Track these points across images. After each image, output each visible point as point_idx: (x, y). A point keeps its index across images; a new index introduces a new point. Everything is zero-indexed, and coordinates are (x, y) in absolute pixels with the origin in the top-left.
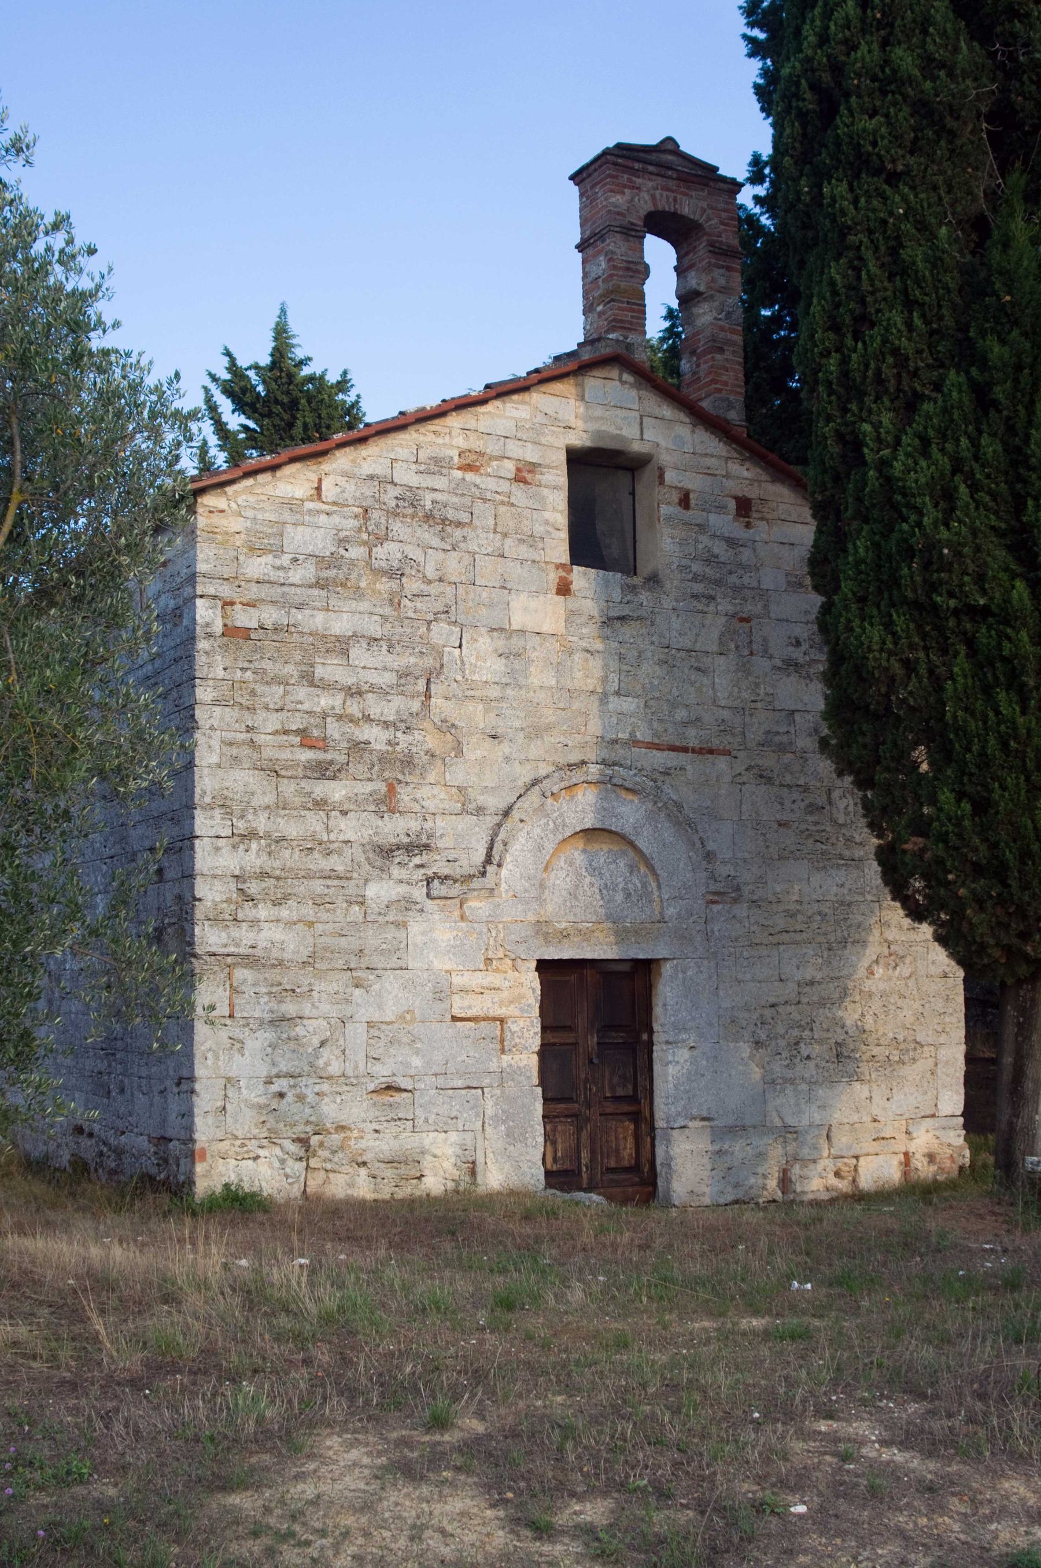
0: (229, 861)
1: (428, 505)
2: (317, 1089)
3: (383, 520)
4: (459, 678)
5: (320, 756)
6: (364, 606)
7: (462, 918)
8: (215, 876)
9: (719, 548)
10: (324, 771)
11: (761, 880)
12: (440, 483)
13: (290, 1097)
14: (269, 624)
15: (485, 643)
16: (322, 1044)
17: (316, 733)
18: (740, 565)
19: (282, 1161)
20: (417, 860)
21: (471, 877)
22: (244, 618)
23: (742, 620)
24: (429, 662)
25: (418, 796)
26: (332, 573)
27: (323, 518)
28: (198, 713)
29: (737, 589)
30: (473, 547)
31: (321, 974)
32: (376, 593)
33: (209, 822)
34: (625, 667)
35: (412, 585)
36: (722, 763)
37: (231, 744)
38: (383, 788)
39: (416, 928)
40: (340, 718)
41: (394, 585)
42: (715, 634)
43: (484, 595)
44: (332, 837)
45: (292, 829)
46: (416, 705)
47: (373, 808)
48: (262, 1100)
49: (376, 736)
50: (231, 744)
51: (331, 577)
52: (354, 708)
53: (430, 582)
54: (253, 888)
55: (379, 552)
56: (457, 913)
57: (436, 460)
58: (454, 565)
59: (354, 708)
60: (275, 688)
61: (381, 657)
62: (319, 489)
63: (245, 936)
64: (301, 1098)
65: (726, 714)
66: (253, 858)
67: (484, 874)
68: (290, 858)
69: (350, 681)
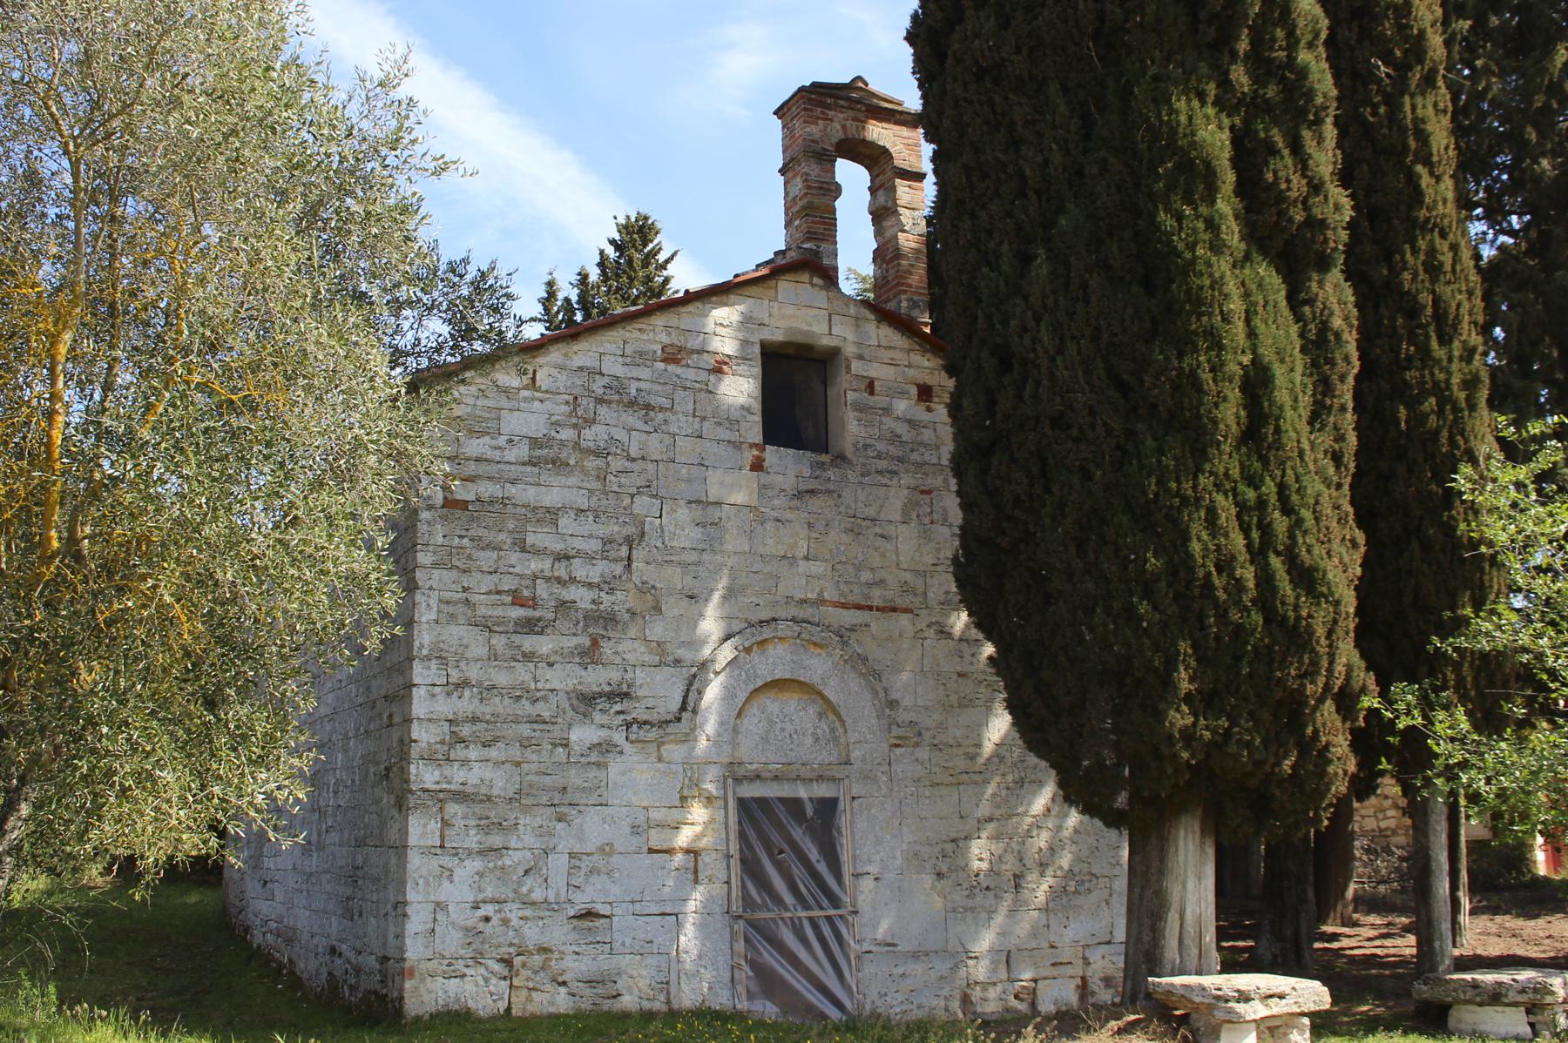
0: (446, 706)
1: (633, 392)
2: (521, 913)
3: (591, 406)
4: (659, 544)
5: (529, 613)
6: (573, 481)
7: (660, 759)
8: (430, 720)
9: (902, 429)
10: (531, 626)
11: (942, 727)
12: (644, 373)
13: (495, 921)
14: (485, 496)
15: (683, 513)
16: (526, 872)
17: (526, 593)
18: (922, 444)
19: (486, 980)
20: (618, 707)
21: (667, 722)
22: (460, 491)
23: (922, 492)
24: (631, 530)
25: (620, 649)
26: (544, 452)
27: (537, 404)
28: (419, 574)
29: (919, 465)
30: (673, 429)
31: (526, 809)
32: (584, 470)
33: (425, 672)
34: (815, 535)
35: (617, 464)
36: (904, 620)
37: (448, 603)
38: (588, 643)
39: (615, 766)
40: (548, 580)
41: (600, 462)
42: (898, 504)
43: (684, 471)
44: (540, 686)
45: (502, 679)
46: (618, 569)
47: (577, 660)
48: (470, 923)
49: (582, 597)
50: (448, 603)
51: (545, 456)
52: (561, 570)
53: (634, 460)
54: (466, 730)
55: (588, 434)
56: (655, 755)
57: (641, 354)
58: (655, 445)
59: (561, 570)
60: (488, 553)
61: (589, 525)
62: (534, 379)
63: (458, 775)
64: (505, 922)
65: (908, 576)
66: (466, 704)
67: (679, 720)
68: (500, 705)
69: (558, 547)
